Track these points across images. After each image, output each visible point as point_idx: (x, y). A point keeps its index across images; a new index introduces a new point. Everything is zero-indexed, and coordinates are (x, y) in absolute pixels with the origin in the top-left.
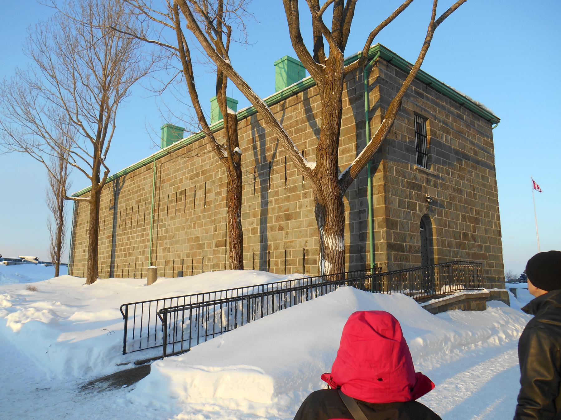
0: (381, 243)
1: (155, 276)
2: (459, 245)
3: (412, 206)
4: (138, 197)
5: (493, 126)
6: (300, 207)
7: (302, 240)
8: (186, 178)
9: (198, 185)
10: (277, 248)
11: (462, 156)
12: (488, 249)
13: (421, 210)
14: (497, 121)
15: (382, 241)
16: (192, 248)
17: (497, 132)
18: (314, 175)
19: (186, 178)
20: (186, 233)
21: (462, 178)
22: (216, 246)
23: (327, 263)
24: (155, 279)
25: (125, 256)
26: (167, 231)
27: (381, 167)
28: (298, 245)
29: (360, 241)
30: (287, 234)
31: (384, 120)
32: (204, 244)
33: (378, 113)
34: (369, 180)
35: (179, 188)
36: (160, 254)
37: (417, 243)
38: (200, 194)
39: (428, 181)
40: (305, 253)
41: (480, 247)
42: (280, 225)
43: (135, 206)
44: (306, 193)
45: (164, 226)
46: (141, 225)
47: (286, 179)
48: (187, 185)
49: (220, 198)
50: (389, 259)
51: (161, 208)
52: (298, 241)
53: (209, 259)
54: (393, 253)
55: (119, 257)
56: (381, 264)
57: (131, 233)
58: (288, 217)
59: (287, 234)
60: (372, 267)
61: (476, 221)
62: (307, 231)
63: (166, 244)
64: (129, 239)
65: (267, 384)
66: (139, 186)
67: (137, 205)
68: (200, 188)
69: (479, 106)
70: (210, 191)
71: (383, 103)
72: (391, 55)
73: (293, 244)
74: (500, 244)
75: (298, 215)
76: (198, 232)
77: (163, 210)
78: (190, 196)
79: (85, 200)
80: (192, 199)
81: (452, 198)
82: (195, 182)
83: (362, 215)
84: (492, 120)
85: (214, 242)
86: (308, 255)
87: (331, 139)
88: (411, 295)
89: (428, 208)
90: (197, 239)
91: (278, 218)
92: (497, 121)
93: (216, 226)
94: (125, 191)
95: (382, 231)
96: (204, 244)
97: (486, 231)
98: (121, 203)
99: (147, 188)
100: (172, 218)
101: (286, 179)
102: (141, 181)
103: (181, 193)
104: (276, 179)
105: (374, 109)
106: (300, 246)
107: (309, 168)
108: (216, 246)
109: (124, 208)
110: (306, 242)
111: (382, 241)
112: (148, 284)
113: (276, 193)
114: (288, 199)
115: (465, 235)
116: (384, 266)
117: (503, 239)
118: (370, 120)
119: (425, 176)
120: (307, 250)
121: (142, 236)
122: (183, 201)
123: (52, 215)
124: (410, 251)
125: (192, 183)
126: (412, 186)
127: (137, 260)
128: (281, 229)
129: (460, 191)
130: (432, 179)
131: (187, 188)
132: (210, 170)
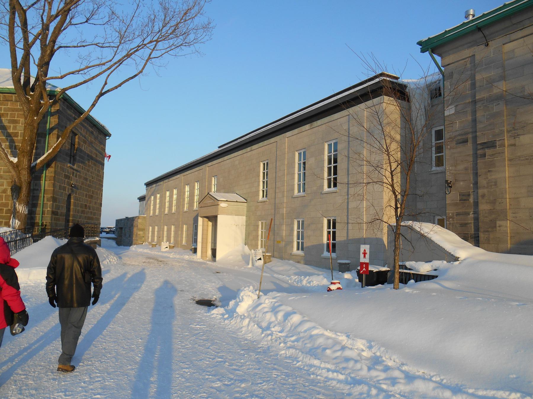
0: (48, 211)
2: (83, 212)
3: (64, 189)
5: (107, 138)
11: (90, 158)
12: (94, 214)
13: (68, 191)
14: (110, 135)
17: (109, 142)
18: (16, 167)
21: (88, 171)
23: (17, 221)
27: (53, 165)
29: (32, 207)
31: (60, 139)
33: (55, 132)
34: (44, 172)
37: (64, 211)
39: (73, 173)
41: (91, 212)
50: (51, 220)
54: (54, 216)
56: (46, 222)
60: (40, 224)
61: (91, 197)
69: (103, 127)
71: (60, 127)
72: (68, 97)
74: (101, 211)
81: (83, 184)
83: (35, 192)
87: (30, 147)
89: (71, 189)
92: (110, 135)
97: (95, 203)
107: (12, 162)
111: (49, 209)
115: (86, 205)
116: (48, 224)
117: (102, 208)
118: (49, 134)
119: (72, 170)
124: (61, 215)
126: (67, 177)
129: (86, 179)
130: (75, 172)
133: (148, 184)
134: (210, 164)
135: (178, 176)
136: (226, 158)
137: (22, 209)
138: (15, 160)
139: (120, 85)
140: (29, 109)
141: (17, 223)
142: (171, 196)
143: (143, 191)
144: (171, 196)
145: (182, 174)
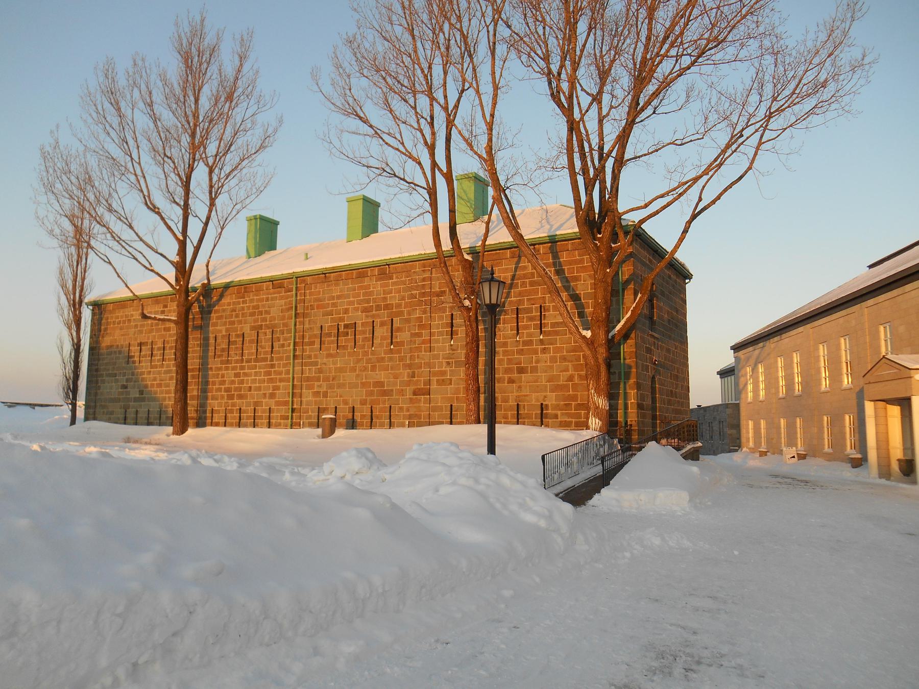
1: (331, 428)
2: (669, 403)
4: (256, 321)
5: (687, 281)
6: (537, 362)
7: (540, 395)
8: (357, 309)
9: (377, 321)
10: (506, 400)
14: (689, 276)
15: (632, 401)
16: (371, 393)
17: (691, 288)
19: (357, 309)
20: (358, 376)
22: (415, 393)
24: (332, 432)
25: (231, 397)
26: (320, 371)
27: (633, 335)
28: (534, 399)
30: (520, 387)
31: (640, 295)
32: (392, 390)
35: (342, 319)
36: (308, 396)
38: (382, 332)
40: (542, 407)
42: (510, 378)
43: (250, 335)
44: (545, 349)
45: (316, 364)
46: (265, 360)
47: (518, 330)
48: (360, 318)
49: (418, 340)
51: (306, 340)
52: (534, 395)
53: (401, 409)
55: (214, 398)
57: (242, 368)
58: (521, 371)
59: (520, 387)
62: (546, 386)
63: (320, 386)
64: (237, 375)
65: (685, 496)
66: (257, 307)
67: (254, 333)
68: (383, 324)
69: (683, 266)
70: (399, 330)
73: (527, 398)
75: (534, 370)
76: (381, 376)
77: (312, 343)
78: (364, 332)
79: (169, 320)
80: (369, 335)
82: (373, 316)
84: (689, 276)
85: (409, 390)
86: (547, 409)
88: (678, 449)
90: (380, 384)
91: (507, 371)
93: (414, 373)
94: (224, 310)
95: (632, 393)
96: (392, 390)
98: (215, 325)
99: (275, 312)
100: (329, 356)
101: (518, 330)
102: (258, 300)
103: (346, 326)
104: (505, 329)
105: (627, 282)
106: (537, 400)
107: (584, 337)
108: (415, 393)
109: (224, 333)
110: (545, 397)
112: (324, 436)
113: (505, 344)
114: (521, 352)
116: (634, 423)
118: (623, 290)
120: (547, 405)
122: (351, 337)
123: (65, 332)
125: (367, 316)
127: (256, 404)
128: (511, 381)
131: (359, 322)
132: (399, 306)
133: (737, 348)
134: (870, 302)
135: (801, 329)
136: (908, 287)
137: (602, 403)
138: (588, 334)
139: (718, 198)
140: (599, 259)
141: (595, 423)
142: (788, 366)
143: (728, 359)
144: (788, 366)
145: (808, 326)
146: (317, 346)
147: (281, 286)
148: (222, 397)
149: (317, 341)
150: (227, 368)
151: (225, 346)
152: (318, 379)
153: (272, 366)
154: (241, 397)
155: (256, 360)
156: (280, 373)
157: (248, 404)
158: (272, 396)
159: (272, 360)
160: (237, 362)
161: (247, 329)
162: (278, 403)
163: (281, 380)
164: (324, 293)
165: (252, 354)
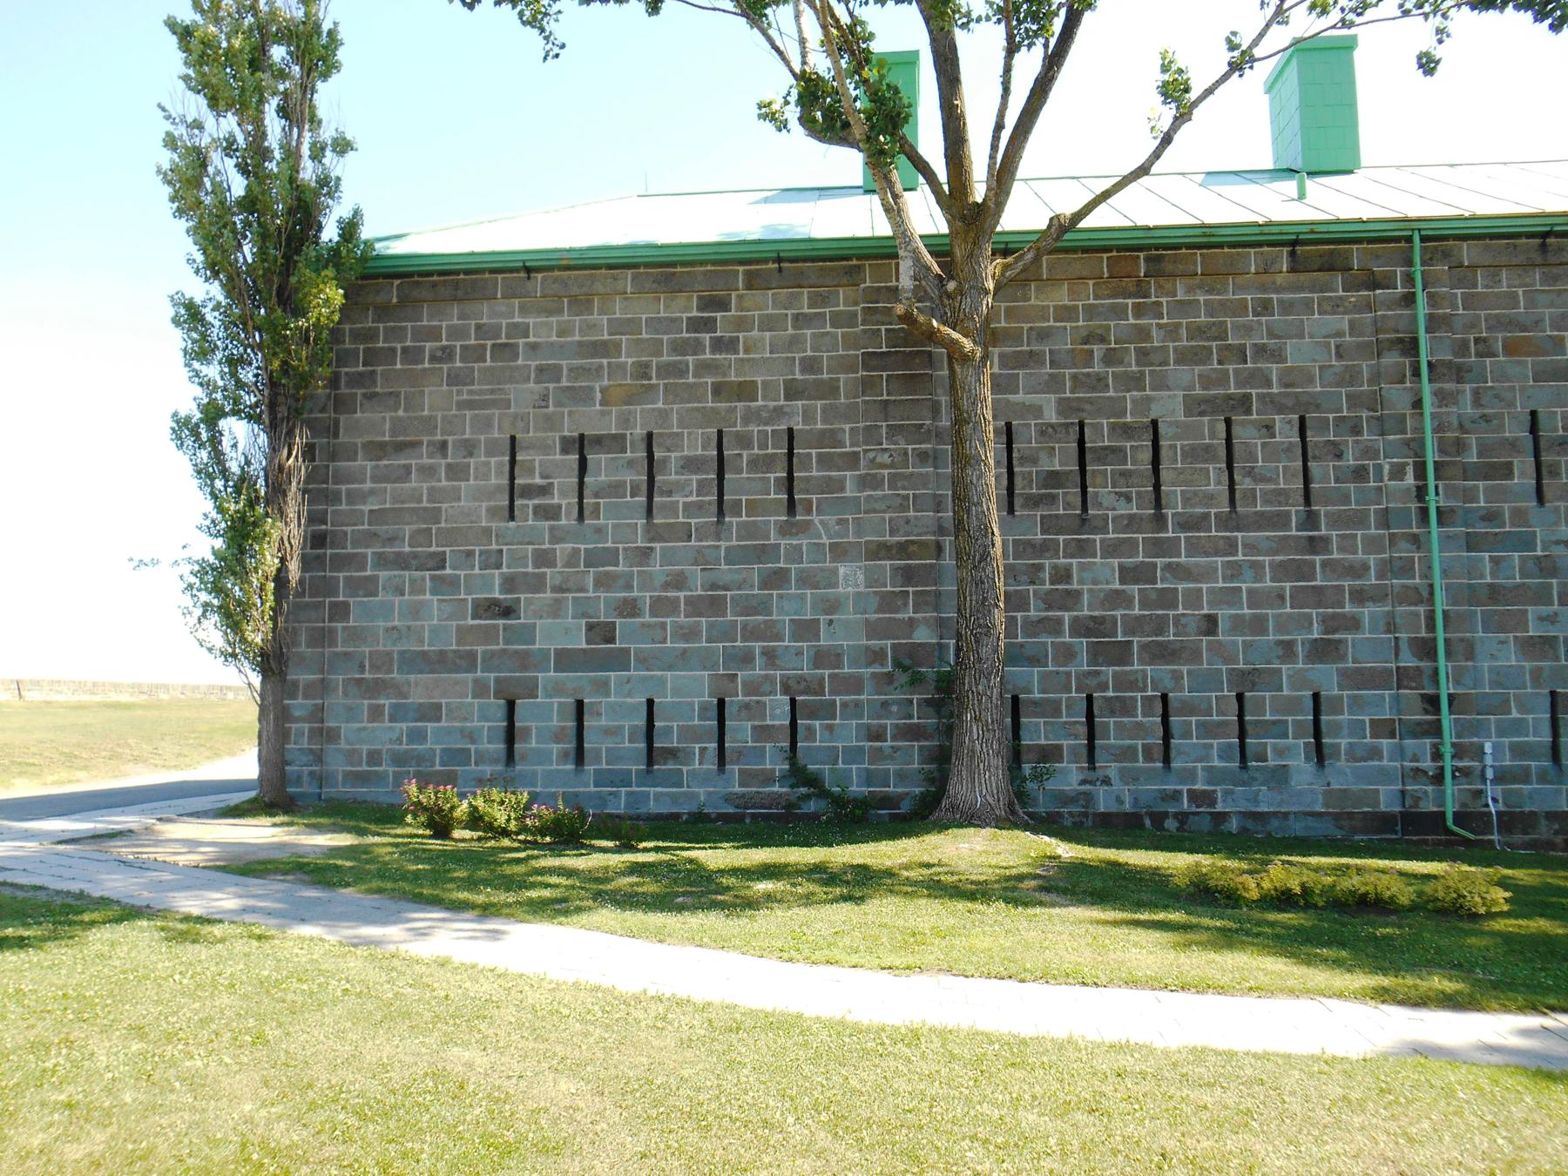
99: (1298, 353)
121: (1303, 571)
146: (1522, 477)
147: (1331, 265)
148: (1067, 654)
149: (1523, 465)
150: (1082, 549)
151: (1061, 460)
152: (1542, 597)
153: (1316, 545)
154: (1161, 653)
155: (1232, 520)
156: (1360, 570)
157: (1212, 681)
158: (1323, 651)
159: (1310, 520)
160: (1132, 523)
161: (1169, 407)
162: (1358, 679)
163: (1360, 596)
164: (1531, 303)
165: (1210, 498)
